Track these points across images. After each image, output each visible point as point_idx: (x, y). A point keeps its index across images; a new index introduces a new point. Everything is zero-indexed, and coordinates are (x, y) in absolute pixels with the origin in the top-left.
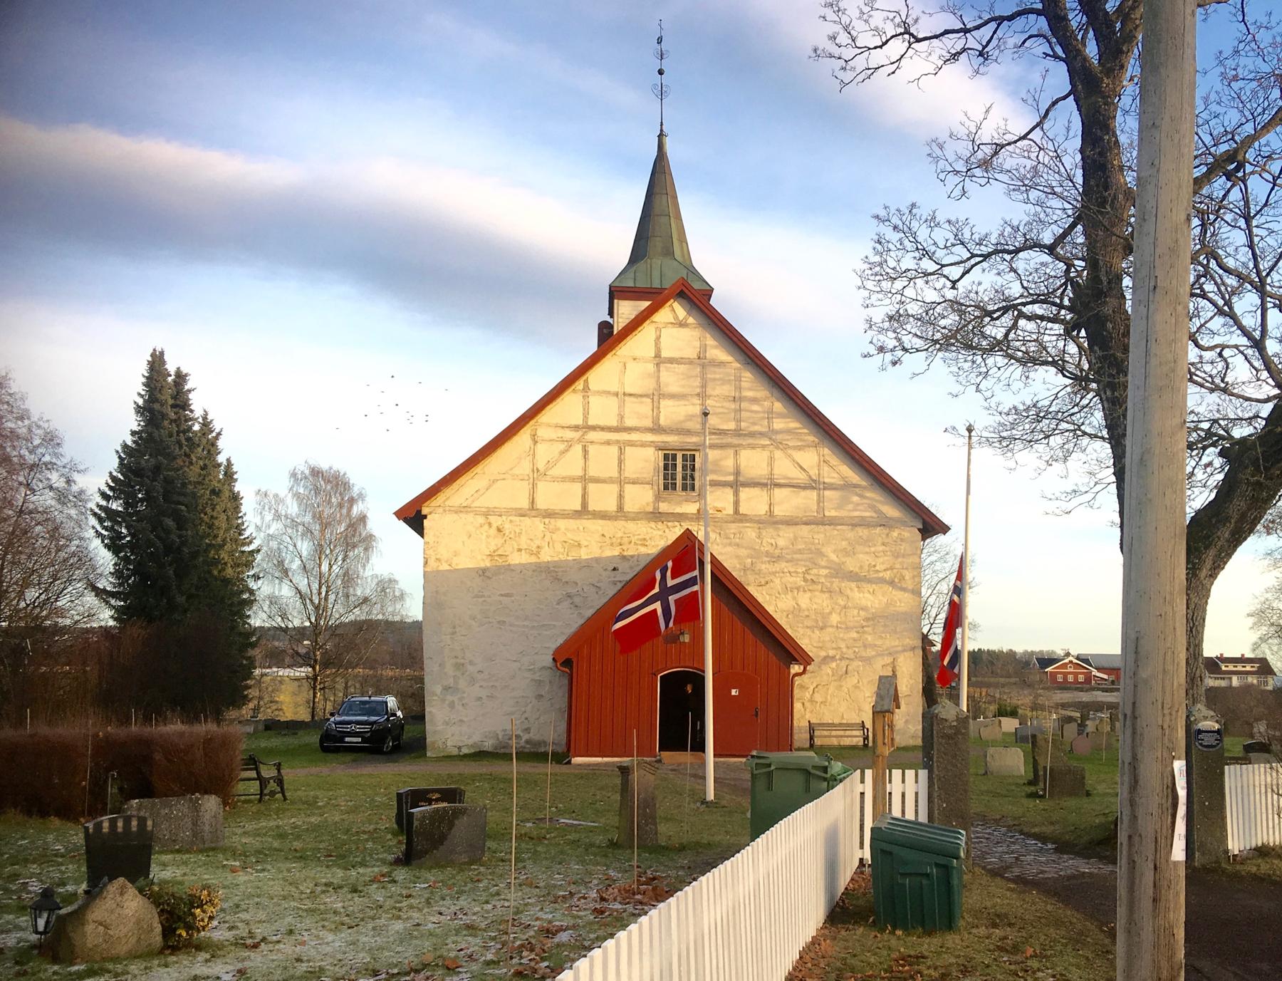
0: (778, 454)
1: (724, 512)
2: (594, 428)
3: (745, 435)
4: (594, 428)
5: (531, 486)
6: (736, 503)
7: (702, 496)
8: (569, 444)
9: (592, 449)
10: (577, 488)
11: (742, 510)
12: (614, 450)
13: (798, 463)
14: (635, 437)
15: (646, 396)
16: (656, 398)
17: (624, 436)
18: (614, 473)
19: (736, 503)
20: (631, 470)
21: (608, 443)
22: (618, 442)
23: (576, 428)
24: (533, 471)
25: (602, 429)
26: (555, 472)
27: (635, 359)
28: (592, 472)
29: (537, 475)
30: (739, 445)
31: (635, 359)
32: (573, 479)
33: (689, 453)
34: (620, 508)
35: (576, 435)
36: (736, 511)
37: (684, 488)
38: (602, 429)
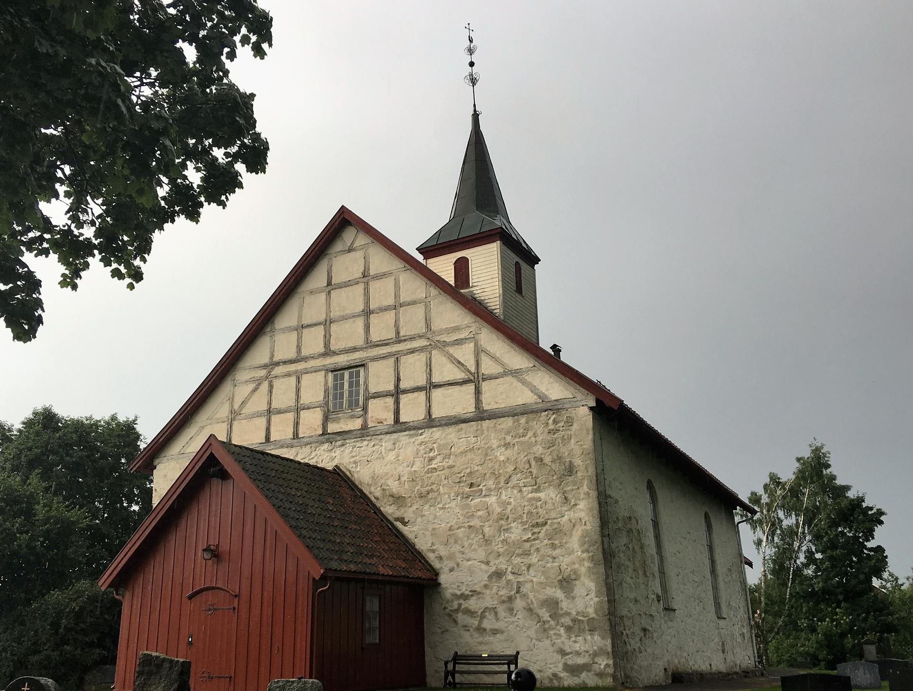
0: (437, 356)
1: (385, 423)
2: (278, 364)
3: (405, 340)
4: (278, 364)
5: (229, 426)
6: (397, 412)
7: (365, 409)
8: (259, 382)
9: (277, 383)
10: (263, 421)
11: (402, 420)
12: (293, 380)
13: (455, 359)
14: (312, 363)
15: (320, 324)
16: (328, 322)
17: (300, 366)
18: (292, 403)
19: (397, 412)
20: (307, 397)
21: (289, 375)
22: (296, 372)
23: (265, 366)
24: (232, 413)
25: (285, 363)
26: (247, 410)
27: (311, 292)
28: (275, 405)
29: (234, 415)
30: (398, 352)
31: (311, 292)
32: (259, 415)
33: (354, 370)
34: (296, 435)
35: (263, 373)
36: (397, 420)
37: (350, 406)
38: (285, 363)
